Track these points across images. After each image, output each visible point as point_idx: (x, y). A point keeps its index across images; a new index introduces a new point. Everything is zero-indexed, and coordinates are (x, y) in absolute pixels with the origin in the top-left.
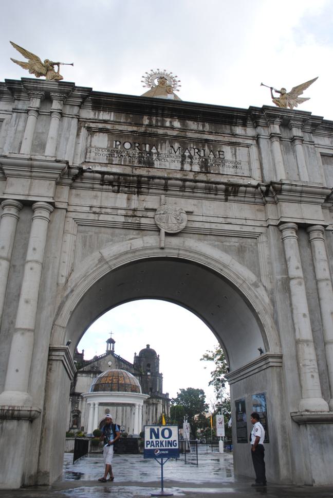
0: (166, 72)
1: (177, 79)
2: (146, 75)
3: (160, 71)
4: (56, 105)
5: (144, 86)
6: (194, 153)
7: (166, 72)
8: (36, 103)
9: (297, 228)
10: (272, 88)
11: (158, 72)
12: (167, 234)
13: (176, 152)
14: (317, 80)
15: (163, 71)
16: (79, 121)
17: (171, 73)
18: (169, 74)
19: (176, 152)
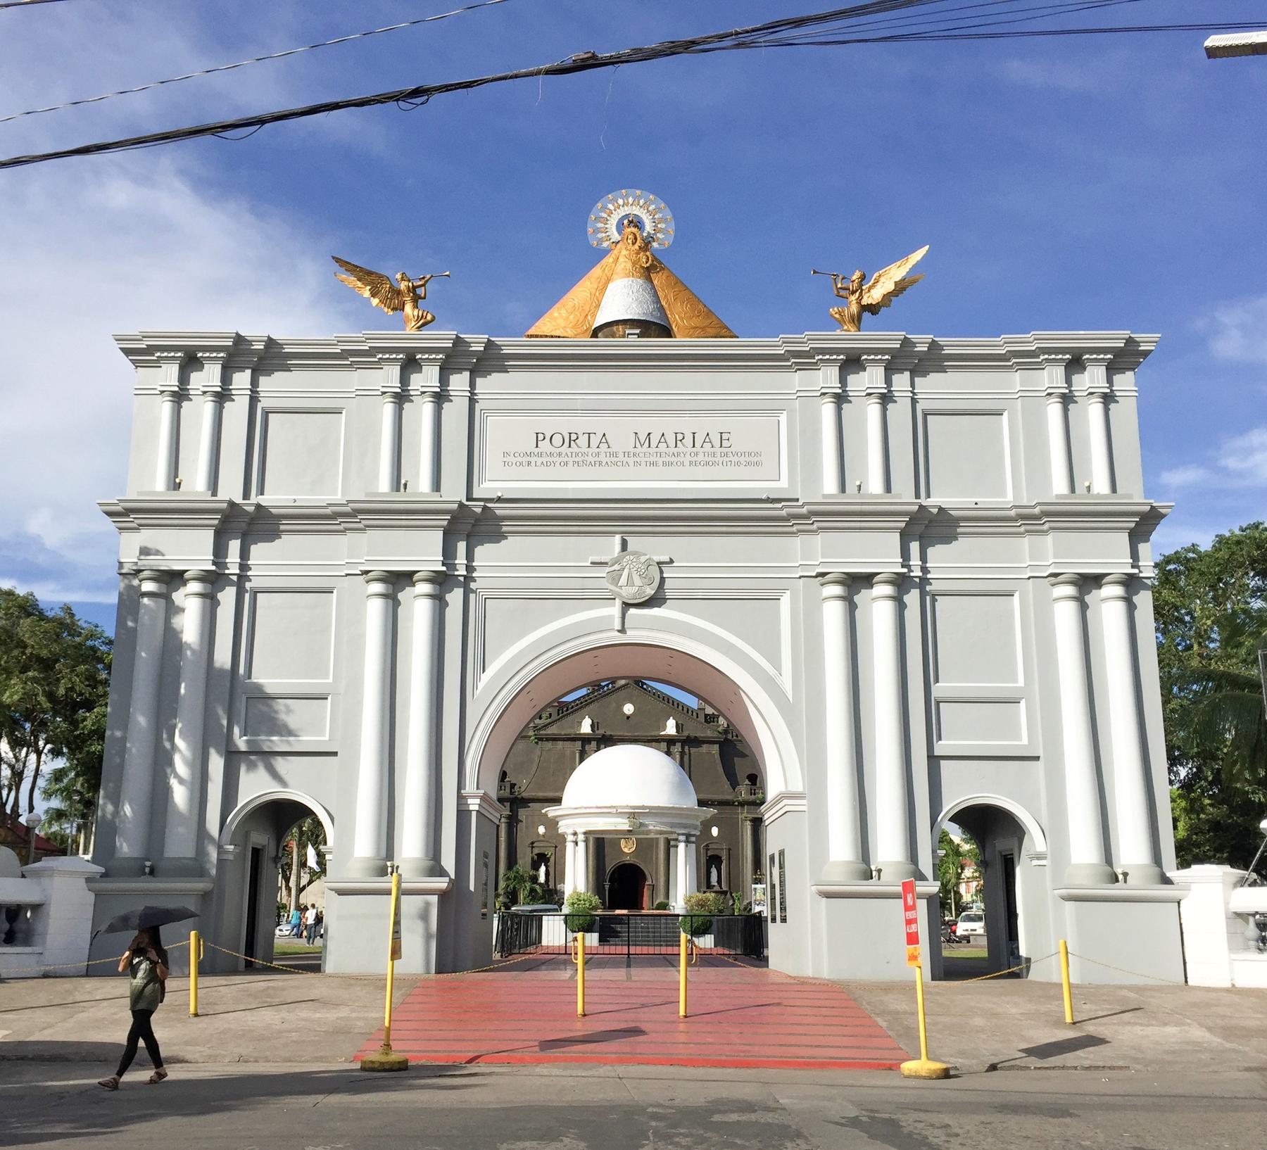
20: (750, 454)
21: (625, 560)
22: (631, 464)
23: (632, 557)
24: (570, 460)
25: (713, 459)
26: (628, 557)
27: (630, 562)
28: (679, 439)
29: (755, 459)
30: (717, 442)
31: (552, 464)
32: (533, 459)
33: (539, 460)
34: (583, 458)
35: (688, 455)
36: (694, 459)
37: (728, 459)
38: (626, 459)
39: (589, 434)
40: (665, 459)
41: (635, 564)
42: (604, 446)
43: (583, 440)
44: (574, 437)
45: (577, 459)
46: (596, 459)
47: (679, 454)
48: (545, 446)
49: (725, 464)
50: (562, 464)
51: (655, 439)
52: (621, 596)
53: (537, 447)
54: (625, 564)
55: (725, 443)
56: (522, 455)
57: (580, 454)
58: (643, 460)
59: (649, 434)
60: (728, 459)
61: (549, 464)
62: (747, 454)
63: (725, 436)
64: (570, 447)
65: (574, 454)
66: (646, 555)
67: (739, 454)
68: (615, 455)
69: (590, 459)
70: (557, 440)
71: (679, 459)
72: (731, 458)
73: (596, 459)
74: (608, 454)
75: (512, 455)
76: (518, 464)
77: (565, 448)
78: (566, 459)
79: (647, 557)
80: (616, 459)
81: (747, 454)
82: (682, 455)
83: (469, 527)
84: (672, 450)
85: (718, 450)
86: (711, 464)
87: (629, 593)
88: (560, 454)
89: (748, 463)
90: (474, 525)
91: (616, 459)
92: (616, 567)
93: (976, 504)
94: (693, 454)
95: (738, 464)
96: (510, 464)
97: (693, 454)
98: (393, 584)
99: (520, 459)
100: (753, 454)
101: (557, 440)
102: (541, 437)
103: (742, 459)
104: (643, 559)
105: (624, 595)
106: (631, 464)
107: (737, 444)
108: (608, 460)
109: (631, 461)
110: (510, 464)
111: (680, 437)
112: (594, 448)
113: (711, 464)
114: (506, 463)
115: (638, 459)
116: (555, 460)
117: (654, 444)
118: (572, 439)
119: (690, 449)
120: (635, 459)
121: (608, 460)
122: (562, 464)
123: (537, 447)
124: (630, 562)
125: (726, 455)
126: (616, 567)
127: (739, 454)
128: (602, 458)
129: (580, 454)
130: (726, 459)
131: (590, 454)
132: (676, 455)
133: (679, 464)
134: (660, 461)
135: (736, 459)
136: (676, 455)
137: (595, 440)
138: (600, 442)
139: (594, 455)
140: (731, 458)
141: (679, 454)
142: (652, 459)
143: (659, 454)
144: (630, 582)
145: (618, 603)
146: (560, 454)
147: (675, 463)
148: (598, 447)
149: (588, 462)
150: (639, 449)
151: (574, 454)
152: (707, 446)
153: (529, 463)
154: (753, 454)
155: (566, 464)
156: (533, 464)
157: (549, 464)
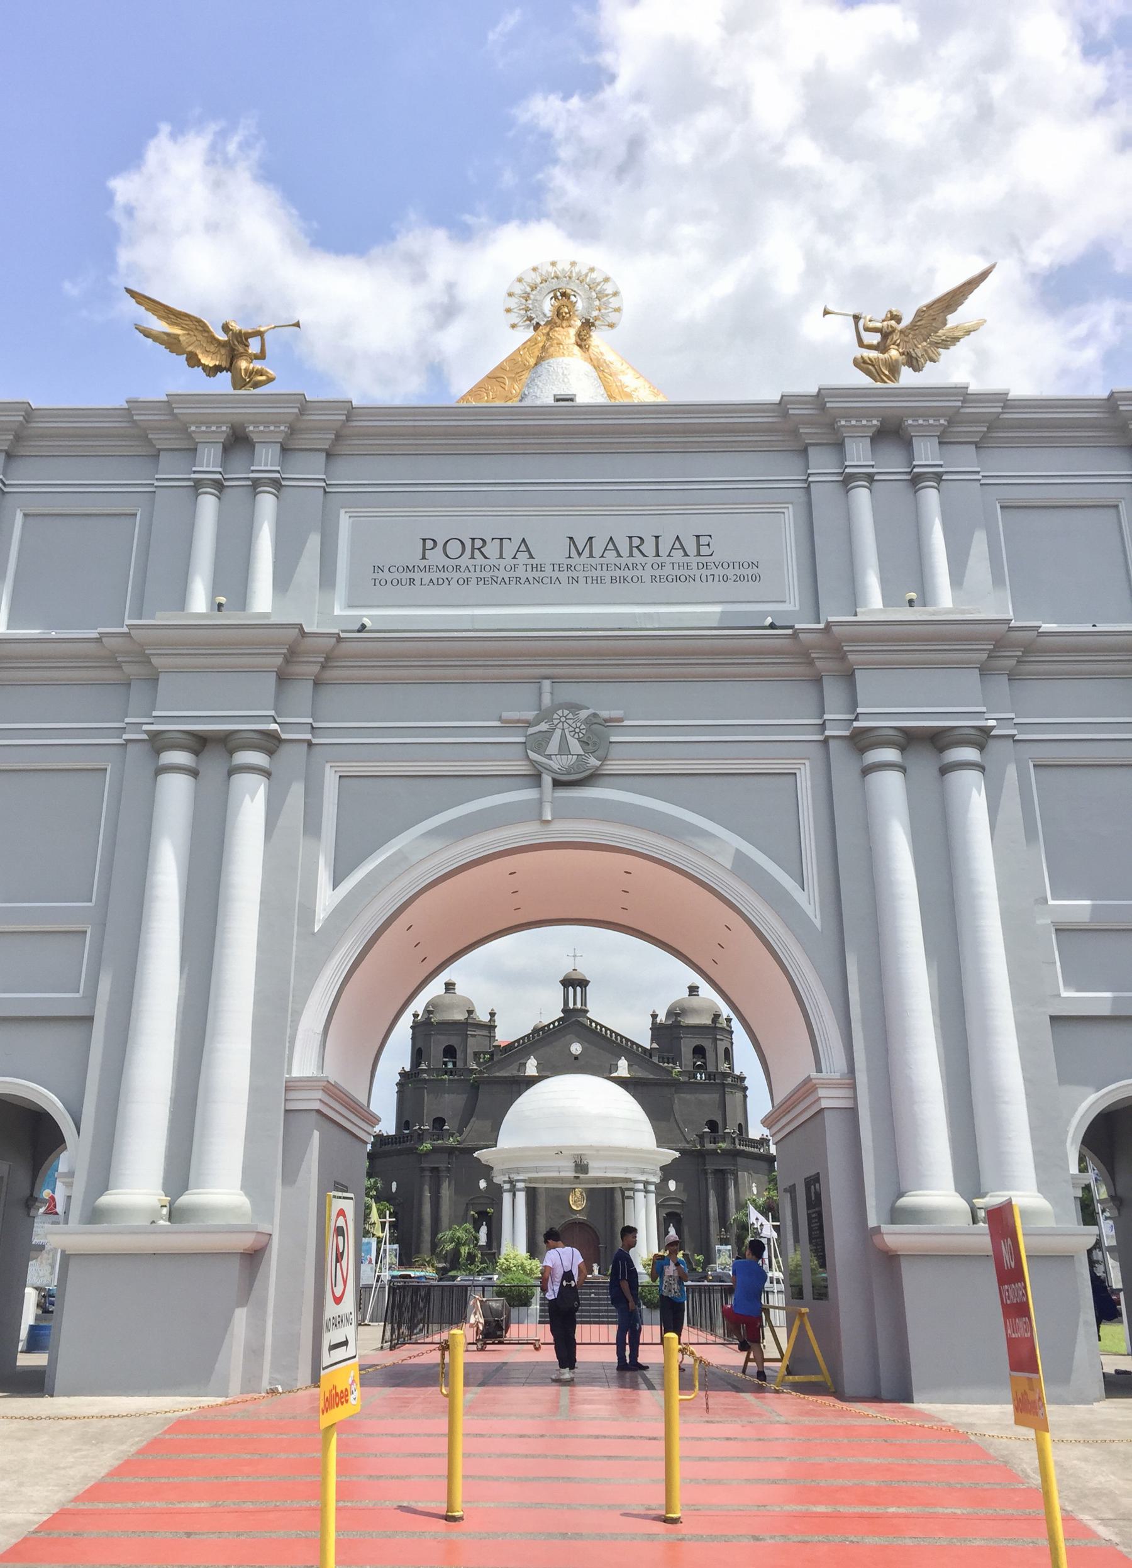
0: (577, 269)
1: (609, 288)
2: (518, 289)
3: (559, 267)
4: (266, 460)
5: (513, 326)
6: (631, 547)
7: (577, 269)
8: (209, 462)
9: (902, 740)
10: (857, 318)
11: (550, 269)
12: (557, 784)
13: (580, 554)
14: (995, 270)
15: (567, 267)
16: (325, 492)
17: (592, 270)
18: (586, 275)
19: (580, 554)
20: (741, 565)
21: (555, 716)
22: (564, 580)
23: (566, 712)
24: (473, 575)
25: (687, 572)
26: (560, 712)
27: (563, 719)
28: (636, 544)
29: (750, 572)
30: (691, 548)
31: (446, 582)
32: (417, 576)
33: (427, 577)
34: (491, 573)
35: (648, 567)
36: (657, 573)
37: (709, 572)
38: (556, 574)
39: (501, 539)
40: (614, 574)
41: (570, 722)
42: (523, 557)
43: (492, 549)
44: (478, 543)
45: (482, 575)
46: (512, 574)
47: (635, 566)
48: (436, 557)
49: (704, 579)
50: (461, 581)
51: (598, 547)
52: (550, 770)
53: (424, 558)
54: (556, 722)
55: (704, 550)
56: (401, 569)
57: (487, 568)
58: (581, 574)
59: (591, 538)
60: (709, 572)
61: (441, 581)
62: (736, 565)
63: (703, 540)
64: (473, 557)
65: (478, 568)
66: (588, 709)
67: (725, 565)
68: (540, 568)
69: (502, 574)
70: (454, 549)
71: (635, 572)
72: (714, 571)
73: (512, 574)
74: (529, 567)
75: (386, 570)
76: (395, 582)
77: (465, 561)
78: (466, 575)
79: (591, 711)
80: (542, 574)
81: (736, 565)
82: (640, 567)
83: (316, 669)
84: (623, 561)
85: (693, 560)
86: (683, 579)
87: (559, 763)
88: (458, 568)
89: (740, 578)
90: (324, 667)
91: (542, 574)
92: (544, 727)
93: (1094, 626)
94: (655, 566)
95: (725, 579)
96: (383, 583)
97: (655, 566)
98: (196, 753)
99: (398, 576)
100: (746, 565)
101: (454, 549)
102: (430, 544)
103: (730, 572)
104: (583, 714)
105: (556, 767)
106: (564, 580)
107: (722, 551)
108: (530, 575)
109: (563, 576)
110: (383, 583)
111: (636, 542)
112: (508, 561)
113: (683, 579)
114: (377, 582)
115: (574, 574)
116: (449, 576)
117: (597, 552)
118: (477, 546)
119: (651, 559)
120: (570, 574)
121: (530, 575)
122: (461, 581)
123: (424, 558)
124: (563, 719)
125: (706, 566)
126: (544, 727)
127: (725, 565)
128: (520, 572)
129: (487, 568)
130: (705, 572)
131: (502, 568)
132: (631, 568)
133: (635, 579)
134: (607, 575)
135: (720, 571)
136: (631, 568)
137: (509, 549)
138: (518, 551)
139: (508, 568)
140: (714, 571)
141: (635, 566)
142: (594, 574)
143: (605, 567)
144: (564, 749)
145: (547, 780)
146: (458, 568)
147: (629, 579)
148: (514, 558)
149: (499, 580)
150: (576, 560)
151: (478, 568)
152: (678, 554)
153: (412, 581)
154: (746, 565)
155: (467, 581)
156: (417, 582)
157: (441, 581)
